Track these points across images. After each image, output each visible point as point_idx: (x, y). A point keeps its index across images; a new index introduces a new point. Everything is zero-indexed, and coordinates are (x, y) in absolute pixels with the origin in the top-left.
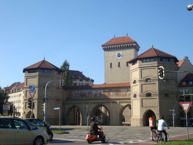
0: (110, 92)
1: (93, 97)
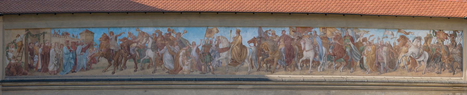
1: (186, 68)
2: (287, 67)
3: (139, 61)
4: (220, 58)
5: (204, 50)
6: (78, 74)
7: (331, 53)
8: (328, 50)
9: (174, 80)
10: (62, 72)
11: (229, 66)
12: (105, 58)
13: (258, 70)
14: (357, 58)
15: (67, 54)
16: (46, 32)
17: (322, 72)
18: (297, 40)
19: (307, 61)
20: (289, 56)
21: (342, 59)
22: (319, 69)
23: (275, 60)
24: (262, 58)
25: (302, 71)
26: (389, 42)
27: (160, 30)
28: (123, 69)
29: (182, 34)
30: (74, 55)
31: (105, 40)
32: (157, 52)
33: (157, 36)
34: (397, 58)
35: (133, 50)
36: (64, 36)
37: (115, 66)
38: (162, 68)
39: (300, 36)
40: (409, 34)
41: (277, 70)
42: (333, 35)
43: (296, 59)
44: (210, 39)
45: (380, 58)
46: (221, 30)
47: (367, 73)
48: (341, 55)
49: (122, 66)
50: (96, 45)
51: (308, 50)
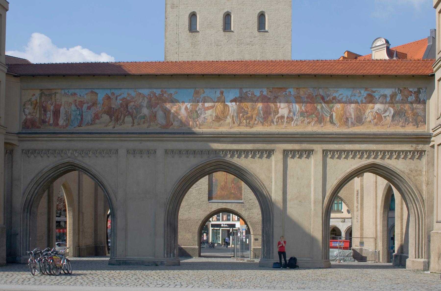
0: (275, 100)
2: (264, 122)
3: (136, 117)
4: (206, 115)
5: (192, 108)
6: (84, 128)
7: (304, 110)
8: (301, 108)
9: (165, 134)
10: (70, 126)
11: (213, 122)
12: (107, 114)
13: (239, 125)
14: (327, 114)
15: (75, 111)
16: (58, 93)
17: (295, 126)
18: (274, 99)
19: (283, 117)
20: (265, 113)
21: (314, 116)
22: (292, 124)
23: (254, 116)
24: (242, 115)
25: (278, 126)
26: (357, 100)
27: (155, 91)
28: (122, 124)
29: (173, 94)
30: (81, 112)
31: (107, 99)
32: (152, 110)
33: (152, 96)
34: (364, 113)
35: (131, 108)
36: (72, 96)
37: (116, 121)
38: (155, 123)
39: (276, 96)
40: (376, 92)
41: (256, 125)
42: (306, 95)
43: (272, 115)
44: (197, 99)
45: (348, 114)
46: (207, 91)
47: (336, 127)
48: (313, 112)
49: (121, 121)
50: (99, 103)
51: (283, 107)
